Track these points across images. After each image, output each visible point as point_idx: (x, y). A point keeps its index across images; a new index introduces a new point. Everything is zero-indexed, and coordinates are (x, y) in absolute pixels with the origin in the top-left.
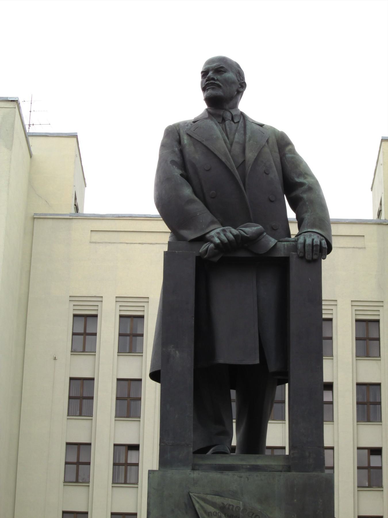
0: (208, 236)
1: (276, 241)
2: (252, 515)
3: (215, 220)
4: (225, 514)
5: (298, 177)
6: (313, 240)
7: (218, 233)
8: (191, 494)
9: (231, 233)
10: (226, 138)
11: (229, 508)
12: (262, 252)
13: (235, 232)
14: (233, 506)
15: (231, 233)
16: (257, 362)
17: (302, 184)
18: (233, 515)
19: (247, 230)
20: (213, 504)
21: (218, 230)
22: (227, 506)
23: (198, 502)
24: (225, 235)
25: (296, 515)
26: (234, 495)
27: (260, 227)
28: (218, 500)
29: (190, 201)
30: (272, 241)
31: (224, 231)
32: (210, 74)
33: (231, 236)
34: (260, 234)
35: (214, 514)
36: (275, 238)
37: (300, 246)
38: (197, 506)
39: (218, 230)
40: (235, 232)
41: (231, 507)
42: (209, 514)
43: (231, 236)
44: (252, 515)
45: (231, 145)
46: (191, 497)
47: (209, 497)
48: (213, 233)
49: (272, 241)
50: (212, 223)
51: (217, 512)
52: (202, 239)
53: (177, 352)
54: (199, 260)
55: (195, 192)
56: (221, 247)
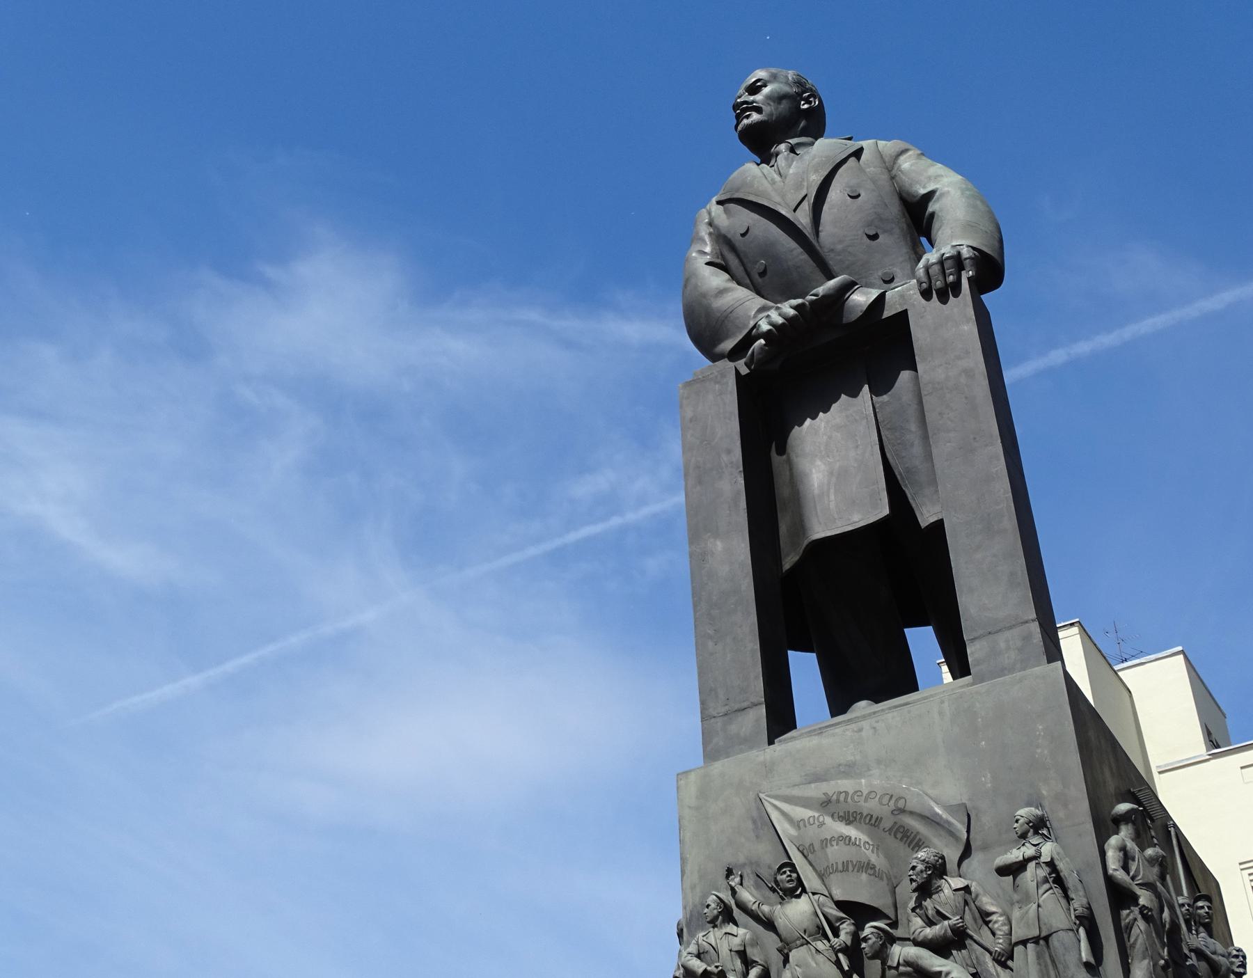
2: (889, 801)
4: (832, 816)
8: (762, 796)
11: (838, 801)
14: (846, 793)
18: (849, 812)
20: (805, 803)
22: (835, 797)
23: (766, 800)
25: (989, 775)
26: (849, 770)
28: (816, 791)
35: (809, 822)
38: (775, 816)
41: (842, 798)
42: (797, 824)
44: (889, 801)
46: (763, 801)
47: (796, 792)
51: (816, 815)
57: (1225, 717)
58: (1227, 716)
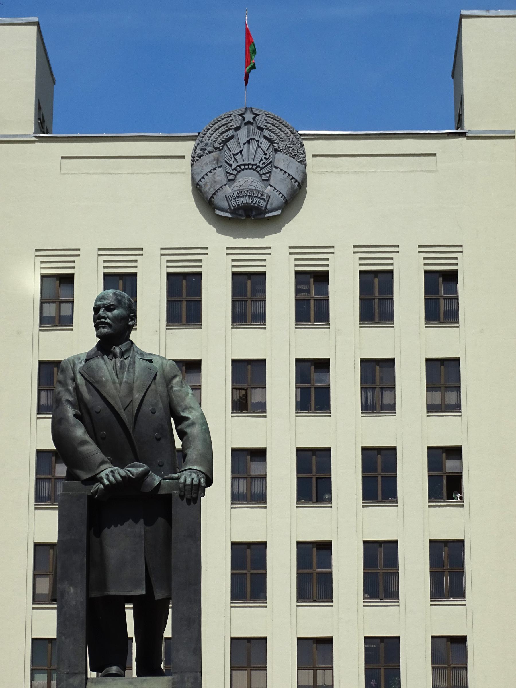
0: (98, 476)
1: (161, 479)
3: (106, 459)
5: (183, 411)
6: (193, 479)
7: (107, 475)
9: (119, 473)
10: (115, 378)
12: (147, 490)
13: (122, 472)
15: (119, 473)
16: (144, 592)
17: (186, 419)
19: (133, 470)
21: (107, 471)
24: (113, 476)
27: (146, 467)
29: (84, 443)
30: (157, 479)
31: (112, 472)
32: (101, 312)
33: (119, 477)
34: (145, 474)
36: (160, 476)
37: (181, 485)
39: (107, 471)
40: (122, 472)
43: (119, 477)
45: (120, 384)
48: (103, 475)
49: (157, 479)
50: (103, 463)
52: (95, 479)
53: (71, 588)
54: (91, 498)
55: (88, 431)
56: (110, 488)
57: (55, 84)
58: (56, 82)
